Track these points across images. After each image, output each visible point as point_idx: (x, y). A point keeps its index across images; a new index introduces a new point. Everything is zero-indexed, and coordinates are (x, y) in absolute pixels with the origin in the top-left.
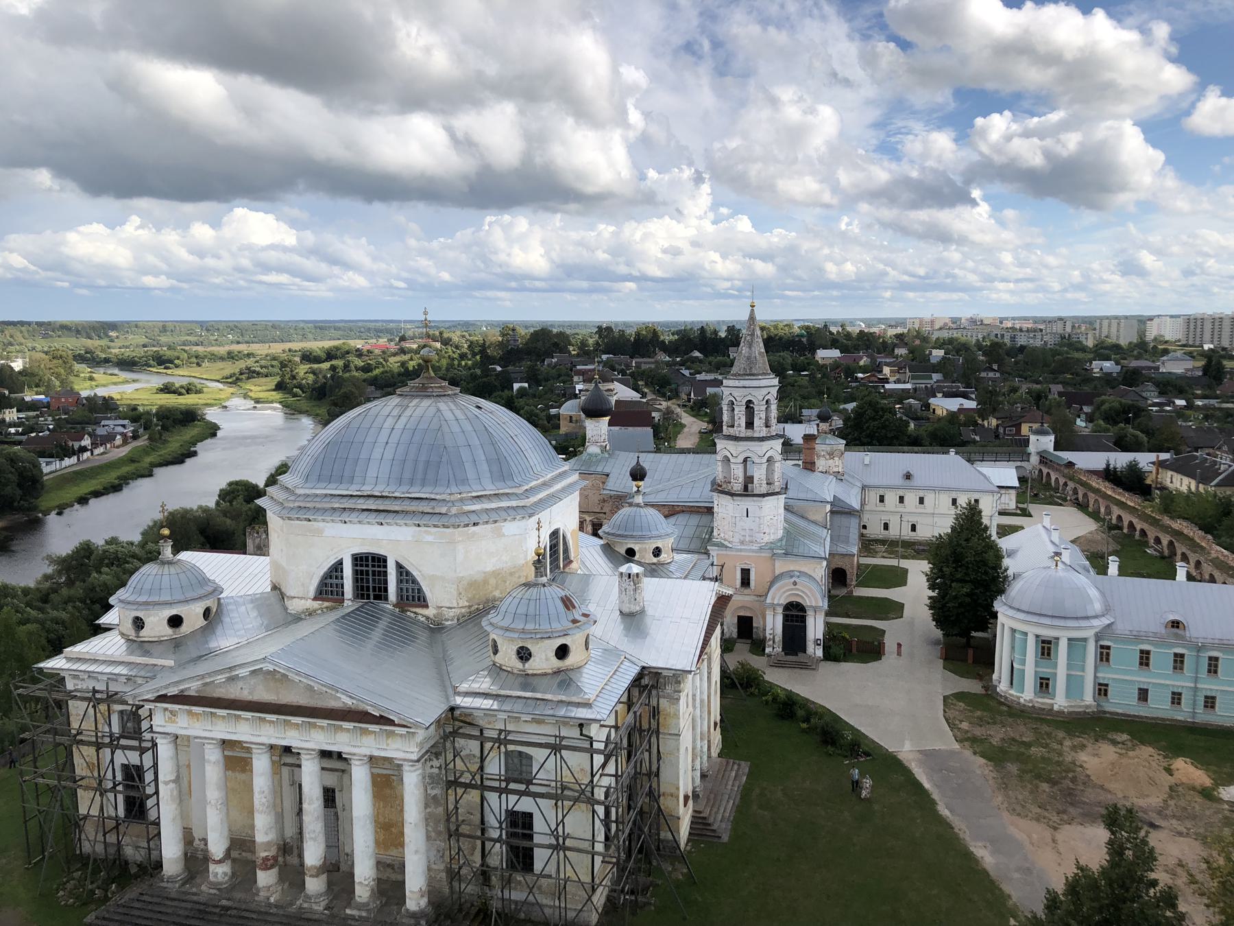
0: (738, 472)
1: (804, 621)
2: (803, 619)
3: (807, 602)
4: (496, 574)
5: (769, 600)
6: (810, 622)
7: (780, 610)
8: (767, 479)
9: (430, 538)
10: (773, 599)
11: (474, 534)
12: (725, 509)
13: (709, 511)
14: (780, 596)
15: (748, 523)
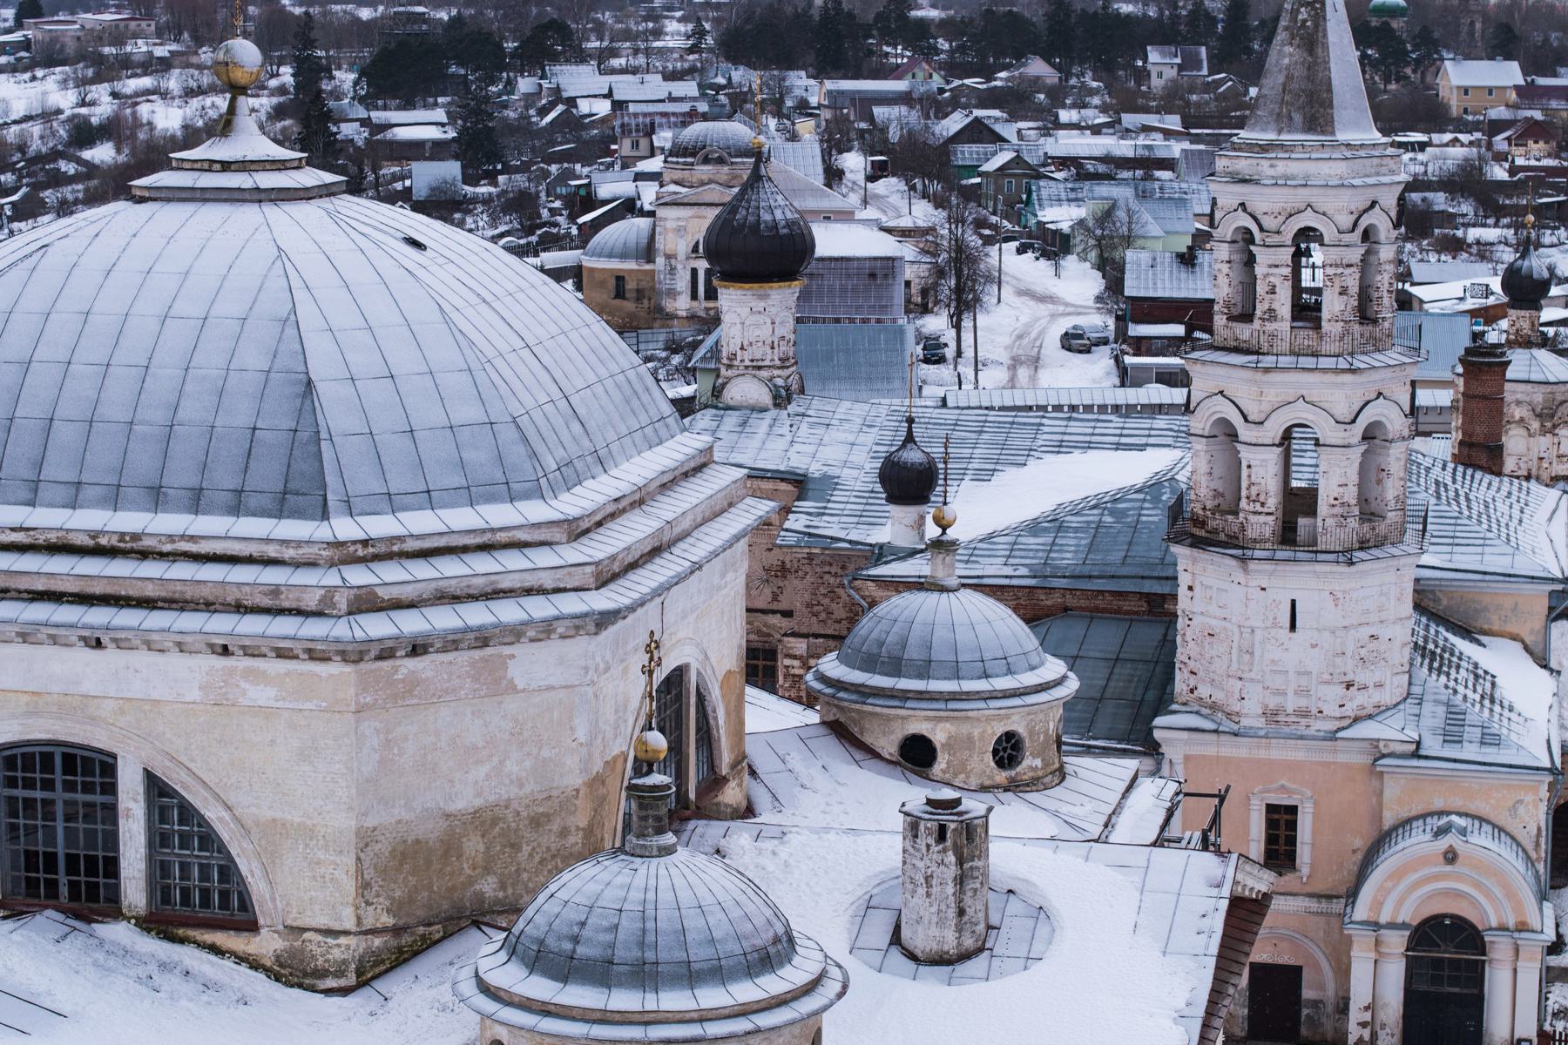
0: (1262, 470)
1: (1479, 981)
2: (1474, 975)
3: (1487, 912)
4: (484, 820)
5: (1361, 911)
6: (1498, 982)
7: (1397, 942)
8: (1363, 500)
9: (261, 695)
10: (1378, 904)
11: (412, 684)
12: (1210, 592)
13: (1158, 608)
14: (1401, 892)
15: (1296, 652)
